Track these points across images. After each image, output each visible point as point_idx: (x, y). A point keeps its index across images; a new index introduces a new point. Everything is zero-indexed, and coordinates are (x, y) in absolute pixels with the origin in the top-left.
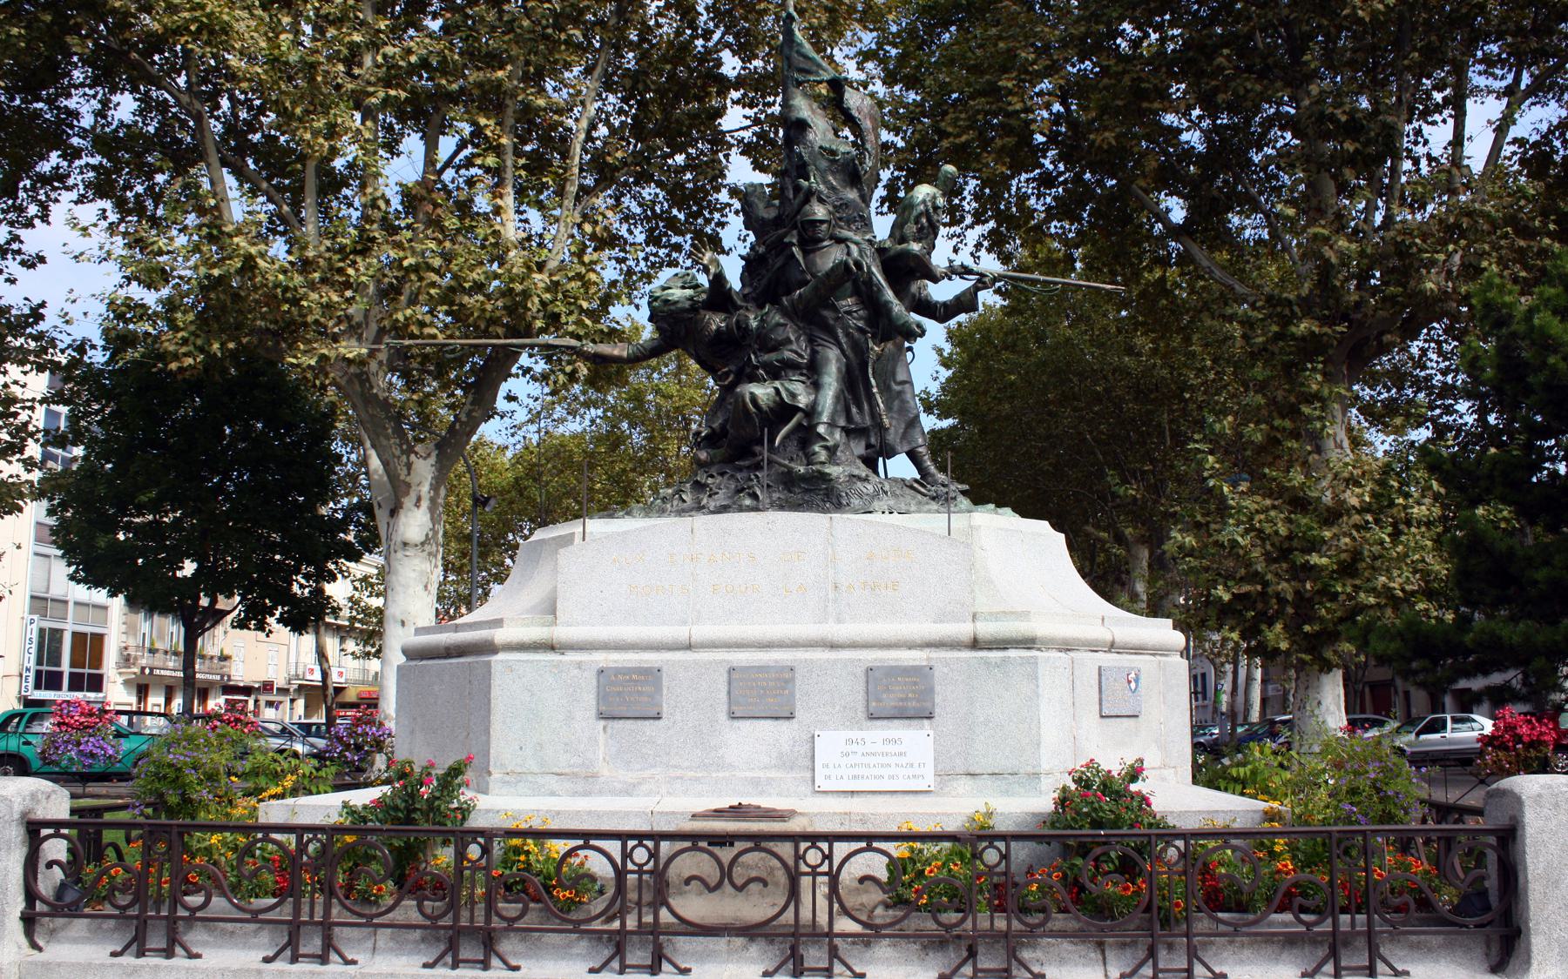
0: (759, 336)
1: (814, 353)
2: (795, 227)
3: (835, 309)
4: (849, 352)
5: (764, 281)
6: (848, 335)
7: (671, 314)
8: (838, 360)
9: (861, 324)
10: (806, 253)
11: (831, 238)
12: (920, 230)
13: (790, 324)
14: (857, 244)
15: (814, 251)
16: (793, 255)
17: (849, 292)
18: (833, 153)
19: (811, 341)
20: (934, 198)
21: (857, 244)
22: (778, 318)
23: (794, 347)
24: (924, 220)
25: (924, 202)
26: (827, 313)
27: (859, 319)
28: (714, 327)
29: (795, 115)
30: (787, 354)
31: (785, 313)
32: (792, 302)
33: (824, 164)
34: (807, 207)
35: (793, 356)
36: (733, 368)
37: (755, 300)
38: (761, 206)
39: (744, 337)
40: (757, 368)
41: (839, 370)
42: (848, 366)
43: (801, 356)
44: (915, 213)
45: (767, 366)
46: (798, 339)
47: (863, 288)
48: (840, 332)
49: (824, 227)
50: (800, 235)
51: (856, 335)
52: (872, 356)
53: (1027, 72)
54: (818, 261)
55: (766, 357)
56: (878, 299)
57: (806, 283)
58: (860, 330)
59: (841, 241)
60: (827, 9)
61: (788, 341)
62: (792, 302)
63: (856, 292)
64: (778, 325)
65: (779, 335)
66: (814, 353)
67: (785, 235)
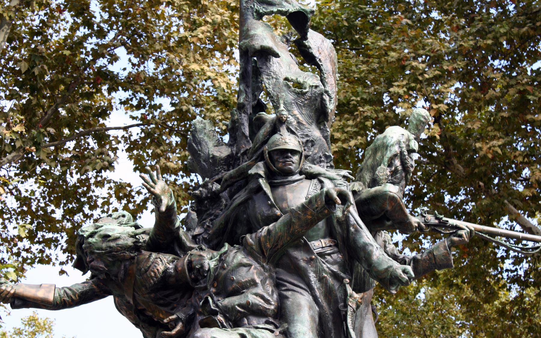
0: (216, 278)
1: (282, 298)
2: (261, 158)
3: (308, 250)
4: (321, 299)
5: (218, 221)
6: (321, 279)
7: (110, 251)
8: (311, 308)
9: (335, 268)
10: (274, 187)
11: (301, 173)
12: (394, 173)
13: (255, 264)
14: (331, 179)
15: (283, 184)
16: (260, 189)
17: (322, 233)
18: (299, 85)
19: (278, 285)
20: (409, 140)
21: (331, 179)
22: (241, 257)
23: (260, 290)
24: (397, 163)
25: (399, 143)
26: (300, 256)
27: (335, 263)
28: (161, 268)
29: (258, 43)
30: (251, 298)
31: (249, 251)
32: (259, 241)
33: (290, 97)
34: (277, 136)
35: (258, 301)
36: (182, 316)
37: (207, 242)
38: (211, 144)
39: (196, 281)
40: (215, 313)
41: (312, 317)
42: (321, 316)
43: (267, 301)
44: (389, 154)
45: (227, 312)
46: (263, 282)
47: (338, 229)
48: (312, 277)
49: (296, 158)
50: (267, 166)
51: (330, 280)
52: (352, 304)
53: (416, 81)
54: (289, 195)
55: (227, 302)
56: (355, 241)
57: (276, 218)
58: (334, 275)
59: (310, 176)
60: (234, 10)
61: (253, 283)
62: (259, 241)
63: (330, 233)
64: (241, 265)
65: (243, 275)
66: (282, 298)
67: (250, 167)
